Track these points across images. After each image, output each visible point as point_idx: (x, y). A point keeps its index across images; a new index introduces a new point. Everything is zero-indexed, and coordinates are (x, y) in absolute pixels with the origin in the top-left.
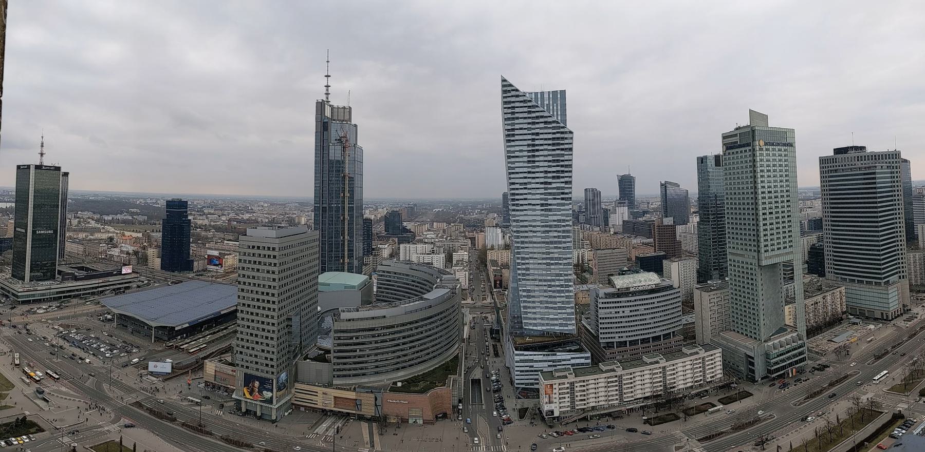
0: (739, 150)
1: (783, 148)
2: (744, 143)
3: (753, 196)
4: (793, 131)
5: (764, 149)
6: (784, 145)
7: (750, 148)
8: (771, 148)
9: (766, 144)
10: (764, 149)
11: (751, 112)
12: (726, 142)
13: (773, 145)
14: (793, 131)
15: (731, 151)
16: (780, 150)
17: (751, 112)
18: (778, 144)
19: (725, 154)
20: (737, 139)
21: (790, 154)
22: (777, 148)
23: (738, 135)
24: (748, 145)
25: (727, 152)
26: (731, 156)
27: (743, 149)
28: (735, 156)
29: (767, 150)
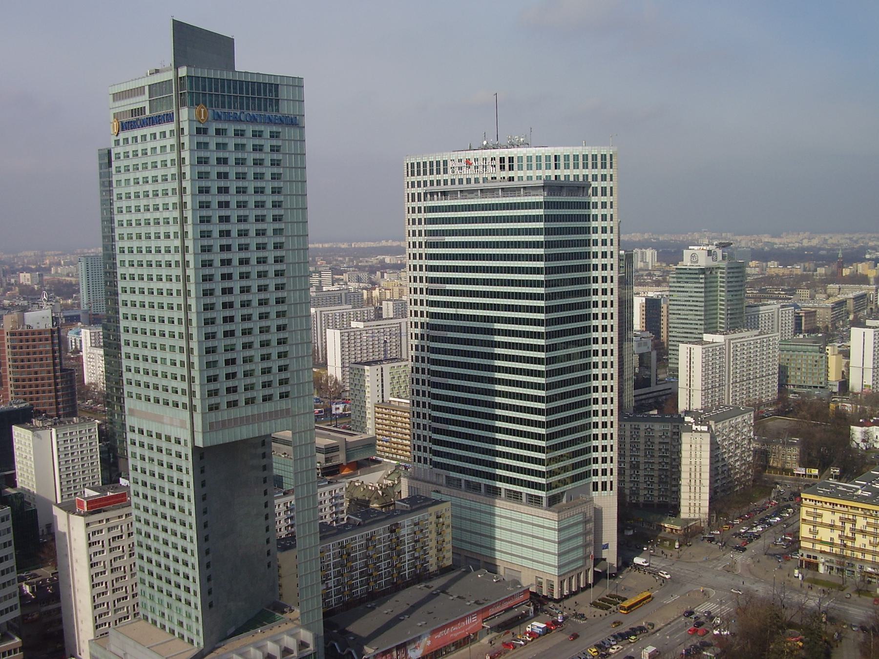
0: (148, 131)
1: (267, 130)
2: (162, 112)
3: (178, 257)
4: (297, 84)
5: (212, 131)
6: (270, 121)
7: (172, 126)
8: (231, 128)
9: (218, 118)
10: (212, 131)
11: (179, 27)
12: (117, 110)
13: (238, 120)
14: (297, 84)
15: (129, 134)
16: (257, 134)
17: (179, 27)
18: (253, 120)
19: (117, 142)
20: (142, 101)
21: (286, 147)
22: (249, 129)
23: (147, 89)
24: (169, 118)
25: (123, 135)
26: (130, 148)
27: (157, 129)
28: (139, 147)
29: (218, 132)
